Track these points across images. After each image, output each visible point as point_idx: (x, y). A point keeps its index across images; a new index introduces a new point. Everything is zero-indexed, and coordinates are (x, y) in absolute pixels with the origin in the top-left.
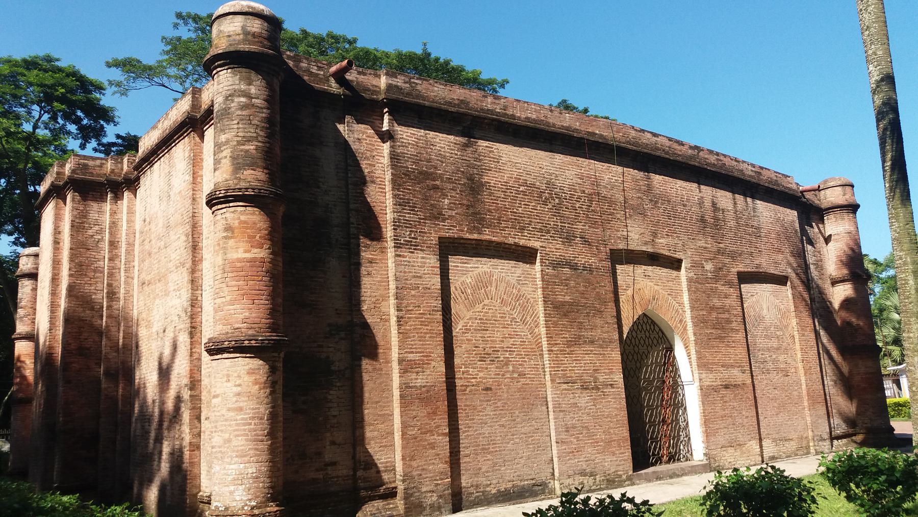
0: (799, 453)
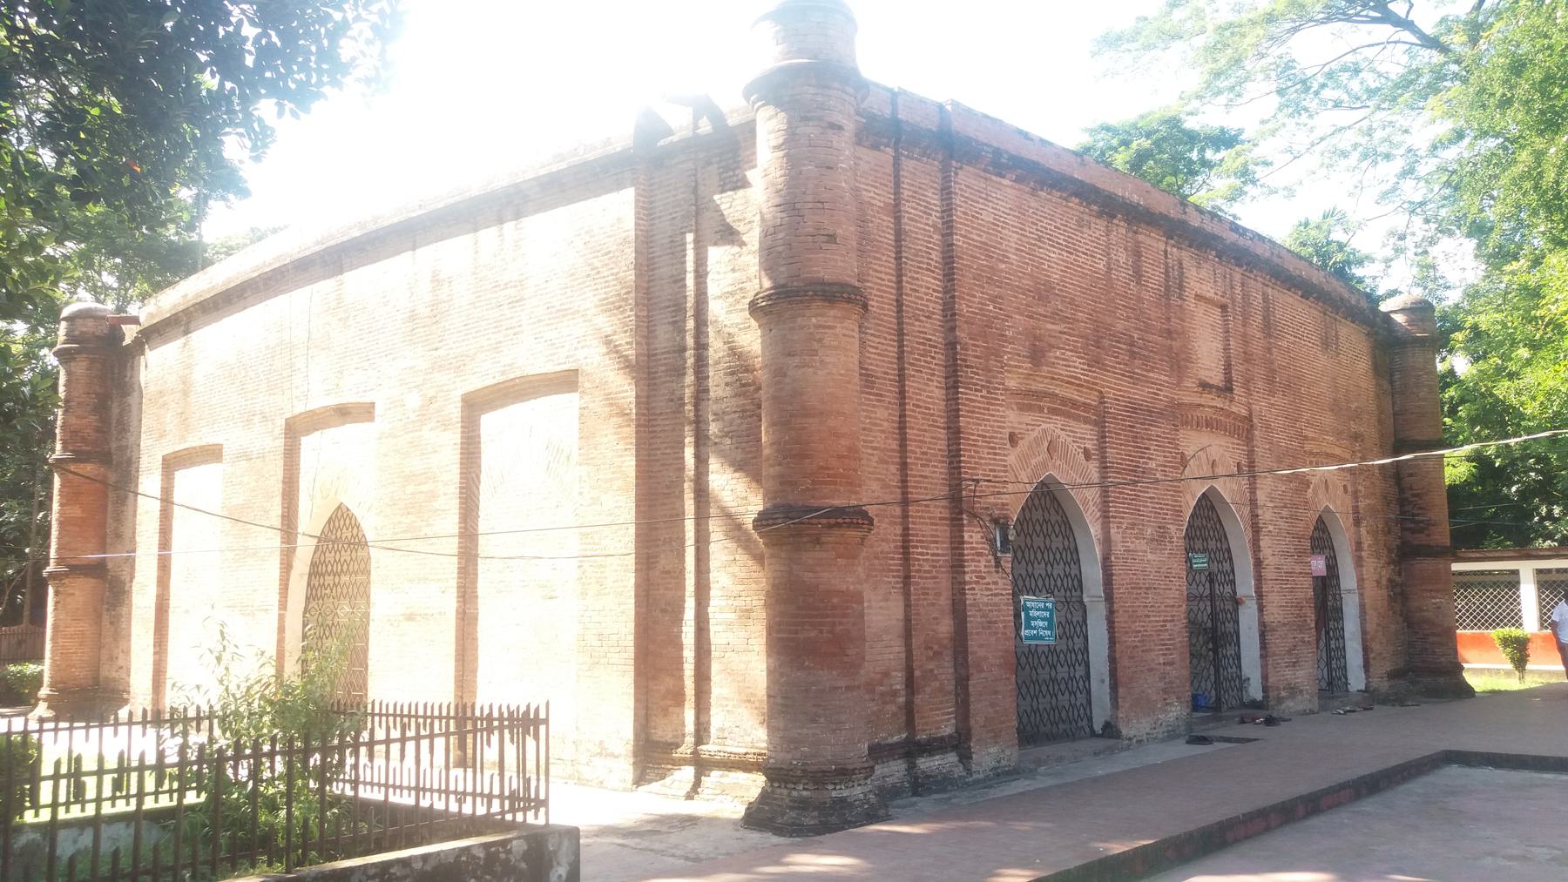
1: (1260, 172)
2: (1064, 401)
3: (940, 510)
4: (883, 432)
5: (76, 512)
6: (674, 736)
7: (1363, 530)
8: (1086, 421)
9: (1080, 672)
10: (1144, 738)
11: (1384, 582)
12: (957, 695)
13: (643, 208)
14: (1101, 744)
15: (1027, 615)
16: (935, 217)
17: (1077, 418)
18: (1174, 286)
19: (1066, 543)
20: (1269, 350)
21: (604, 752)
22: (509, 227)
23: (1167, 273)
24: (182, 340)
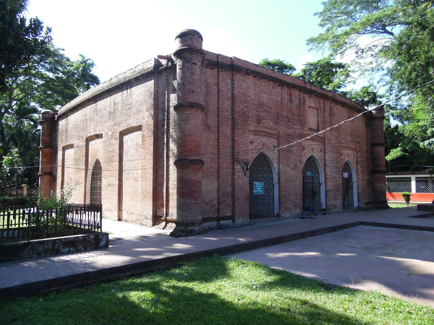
0: (137, 222)
1: (351, 74)
2: (267, 133)
3: (229, 159)
4: (213, 140)
5: (45, 160)
6: (162, 215)
7: (359, 166)
8: (274, 138)
9: (271, 201)
10: (288, 217)
11: (365, 179)
12: (232, 206)
13: (156, 85)
14: (275, 218)
15: (255, 187)
16: (229, 86)
17: (271, 137)
18: (302, 103)
19: (268, 169)
20: (331, 120)
21: (147, 218)
22: (129, 90)
23: (300, 101)
24: (66, 119)
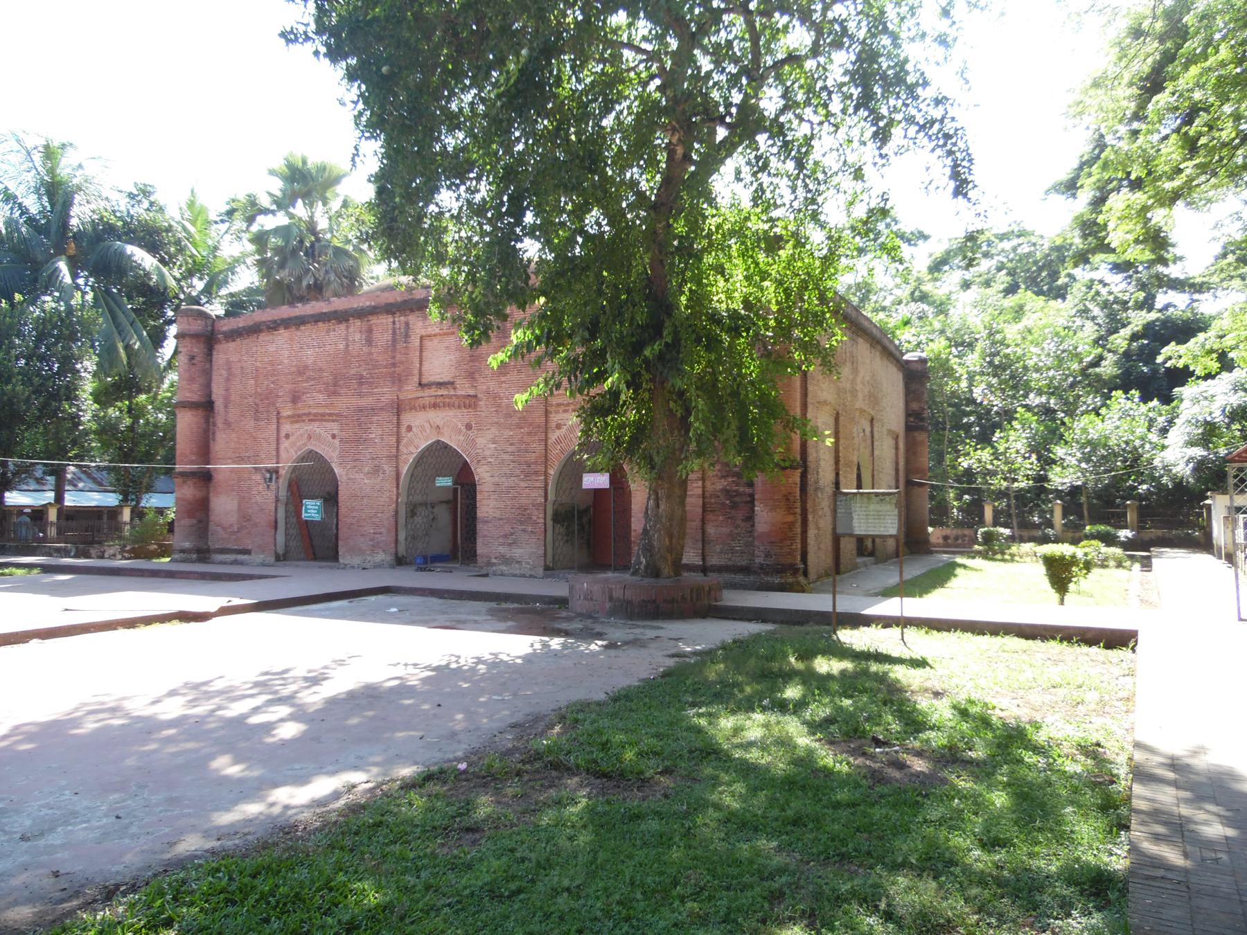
2: (315, 415)
